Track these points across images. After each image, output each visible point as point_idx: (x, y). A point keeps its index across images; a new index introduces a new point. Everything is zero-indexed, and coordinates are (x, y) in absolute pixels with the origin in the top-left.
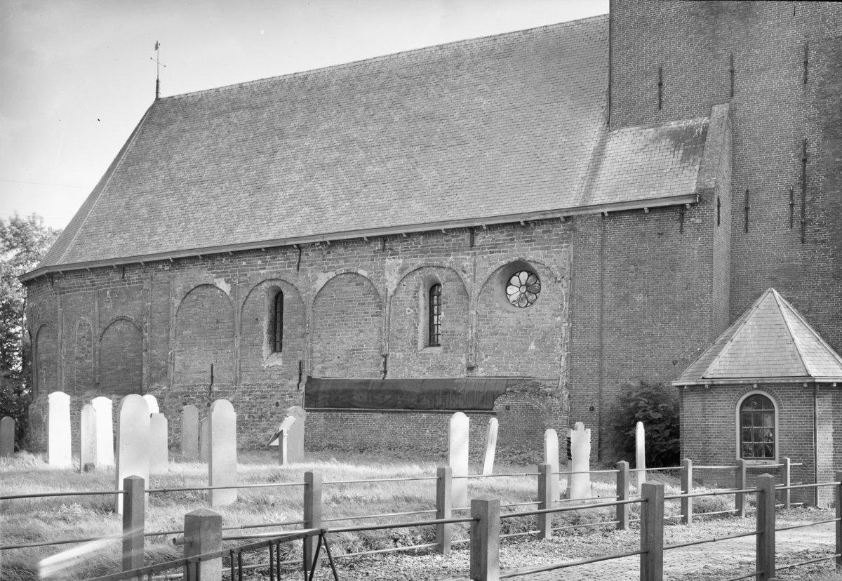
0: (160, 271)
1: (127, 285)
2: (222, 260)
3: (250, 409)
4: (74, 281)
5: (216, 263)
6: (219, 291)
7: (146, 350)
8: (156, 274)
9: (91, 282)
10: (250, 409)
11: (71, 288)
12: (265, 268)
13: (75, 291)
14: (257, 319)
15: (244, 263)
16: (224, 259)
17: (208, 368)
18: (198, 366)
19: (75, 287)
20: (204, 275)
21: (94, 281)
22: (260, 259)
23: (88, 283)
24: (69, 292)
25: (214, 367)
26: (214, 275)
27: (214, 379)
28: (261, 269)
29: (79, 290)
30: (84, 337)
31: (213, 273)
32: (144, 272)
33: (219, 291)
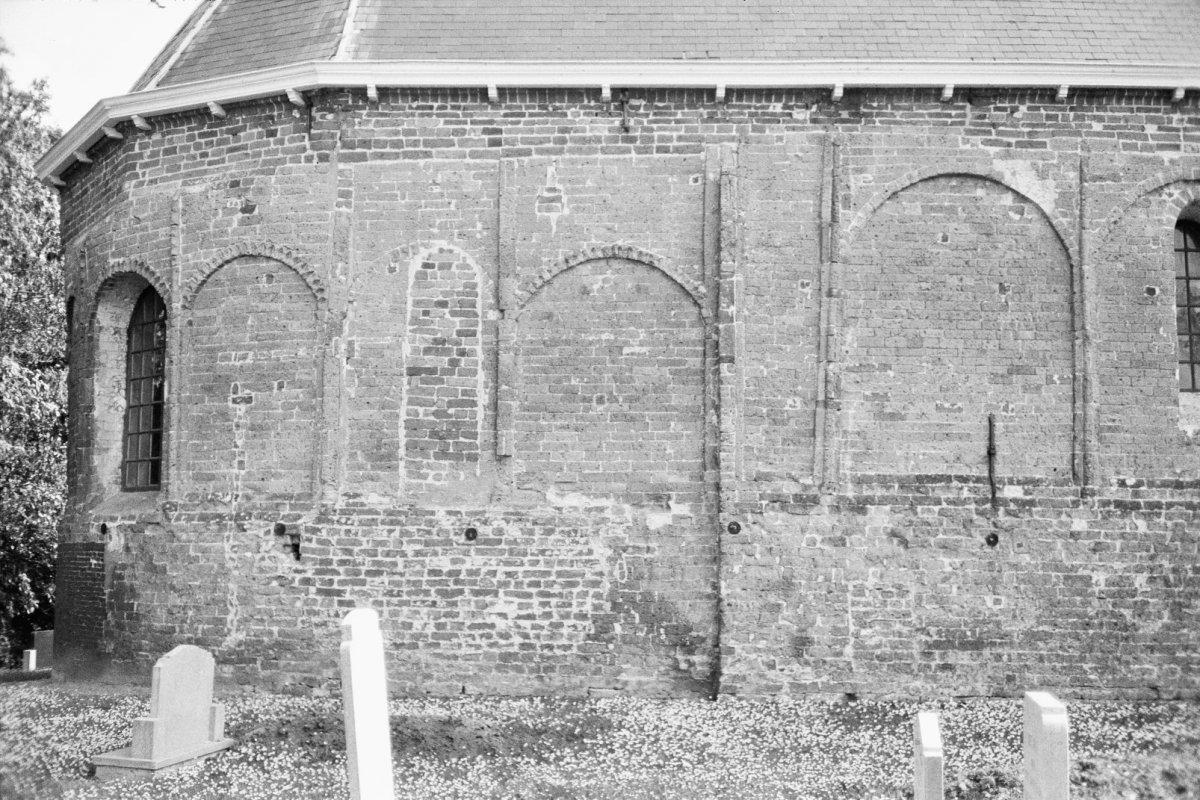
0: (774, 119)
1: (633, 155)
2: (1014, 110)
3: (1152, 558)
4: (417, 122)
5: (992, 113)
6: (1008, 199)
7: (731, 360)
8: (762, 130)
9: (485, 131)
10: (1152, 558)
11: (397, 144)
12: (1177, 147)
13: (415, 155)
14: (1151, 291)
15: (1097, 127)
16: (1023, 109)
17: (975, 425)
18: (936, 418)
19: (415, 143)
20: (965, 144)
21: (500, 131)
22: (1151, 120)
23: (475, 133)
24: (382, 156)
25: (999, 425)
26: (993, 150)
27: (999, 457)
28: (1161, 147)
29: (427, 155)
30: (443, 304)
31: (987, 143)
32: (711, 118)
33: (1008, 199)
